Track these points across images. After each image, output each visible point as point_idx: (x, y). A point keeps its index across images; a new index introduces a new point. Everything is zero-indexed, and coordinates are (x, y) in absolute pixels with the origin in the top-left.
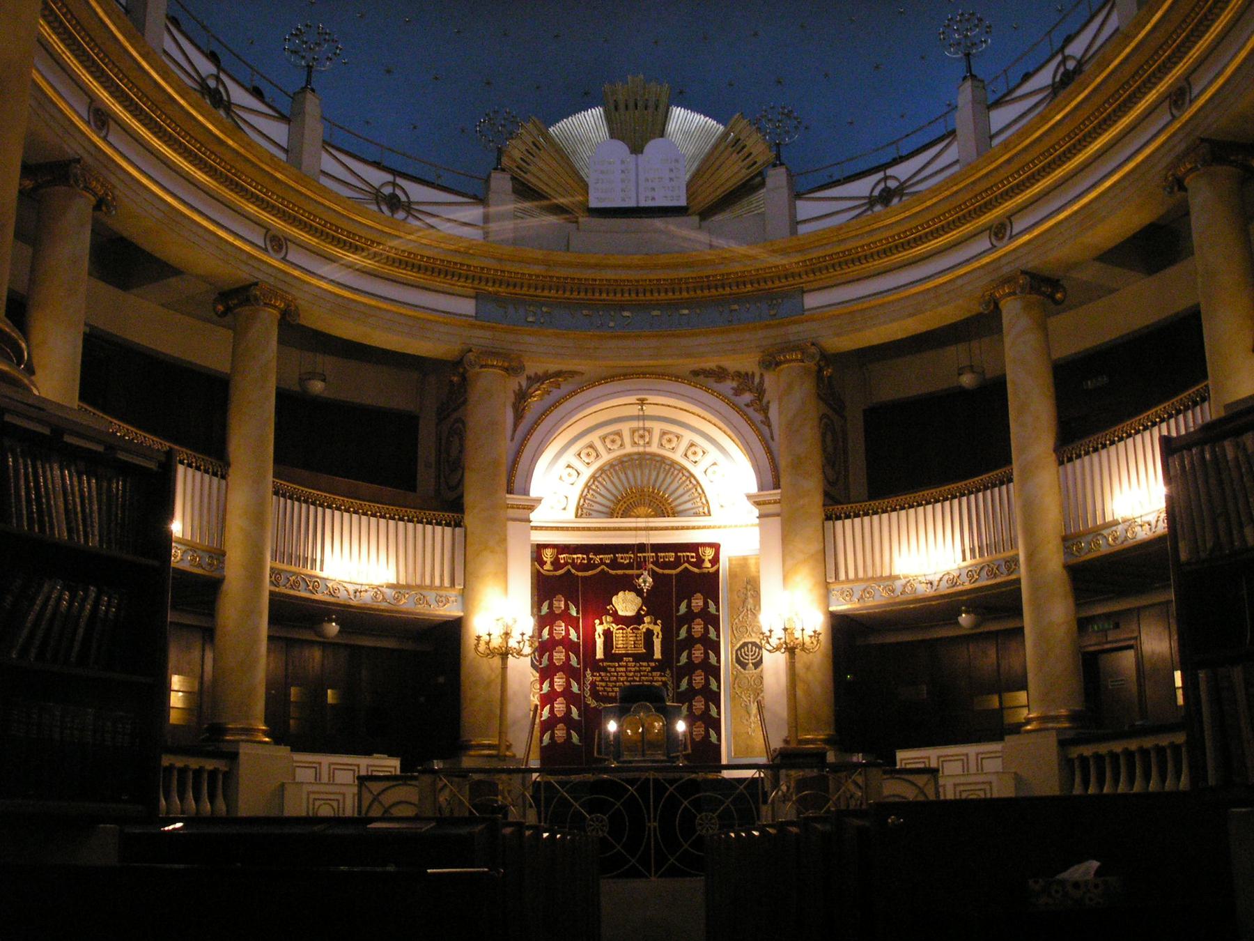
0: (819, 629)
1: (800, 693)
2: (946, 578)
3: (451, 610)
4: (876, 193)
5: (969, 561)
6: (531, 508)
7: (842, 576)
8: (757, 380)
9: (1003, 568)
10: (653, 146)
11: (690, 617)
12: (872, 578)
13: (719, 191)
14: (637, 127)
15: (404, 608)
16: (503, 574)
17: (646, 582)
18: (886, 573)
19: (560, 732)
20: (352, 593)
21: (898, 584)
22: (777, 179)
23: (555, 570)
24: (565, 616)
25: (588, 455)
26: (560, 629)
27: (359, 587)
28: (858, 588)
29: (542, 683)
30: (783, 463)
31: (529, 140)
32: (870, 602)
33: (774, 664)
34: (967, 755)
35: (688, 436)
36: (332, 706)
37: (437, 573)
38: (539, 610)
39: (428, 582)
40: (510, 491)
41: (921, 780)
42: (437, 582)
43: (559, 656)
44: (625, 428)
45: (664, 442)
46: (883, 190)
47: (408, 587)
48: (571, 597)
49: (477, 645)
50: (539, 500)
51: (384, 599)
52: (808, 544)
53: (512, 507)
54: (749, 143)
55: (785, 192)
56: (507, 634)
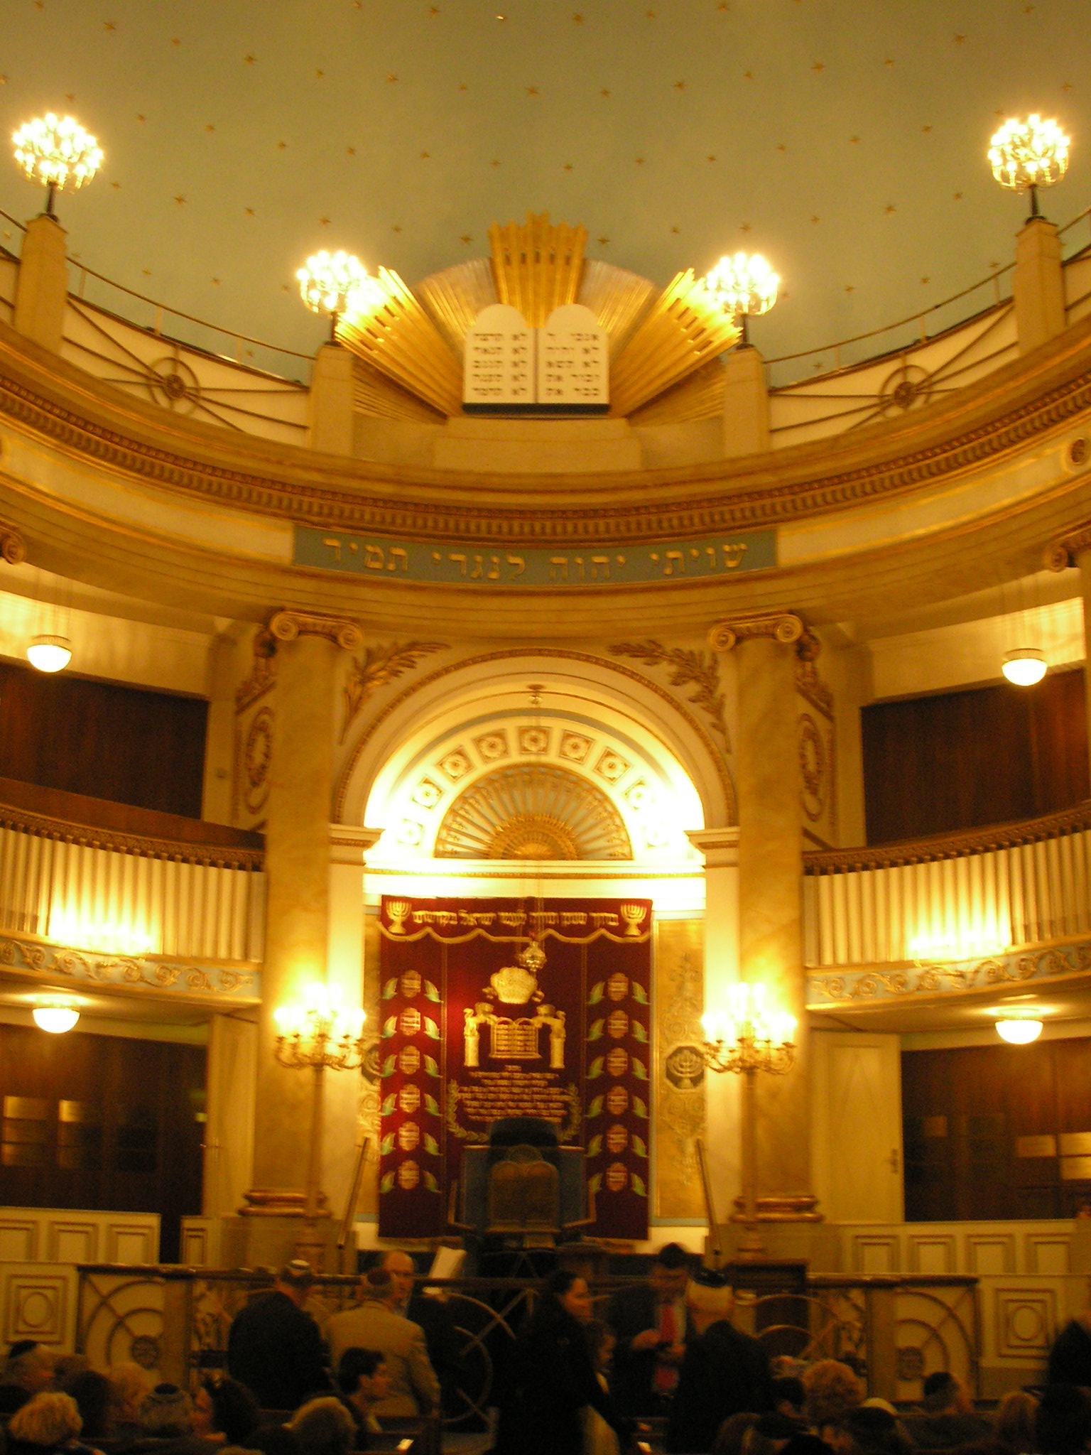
0: (791, 1040)
1: (760, 1132)
2: (987, 968)
3: (243, 995)
4: (890, 391)
5: (1022, 945)
6: (366, 844)
7: (828, 959)
8: (707, 662)
9: (1075, 959)
12: (873, 965)
13: (659, 382)
15: (171, 991)
16: (321, 941)
17: (535, 955)
18: (893, 958)
19: (408, 1174)
20: (92, 967)
21: (912, 974)
23: (407, 934)
24: (421, 1003)
25: (455, 765)
26: (413, 1020)
27: (101, 959)
28: (852, 976)
29: (383, 1100)
30: (743, 788)
32: (869, 1000)
33: (722, 1091)
34: (1010, 1236)
35: (603, 741)
36: (68, 1124)
37: (223, 937)
38: (382, 992)
39: (208, 952)
40: (336, 819)
41: (949, 1296)
42: (223, 953)
43: (410, 1059)
44: (510, 726)
45: (567, 748)
46: (901, 386)
47: (178, 960)
48: (429, 975)
49: (279, 1050)
50: (377, 834)
51: (142, 979)
52: (777, 909)
53: (339, 842)
56: (323, 1037)
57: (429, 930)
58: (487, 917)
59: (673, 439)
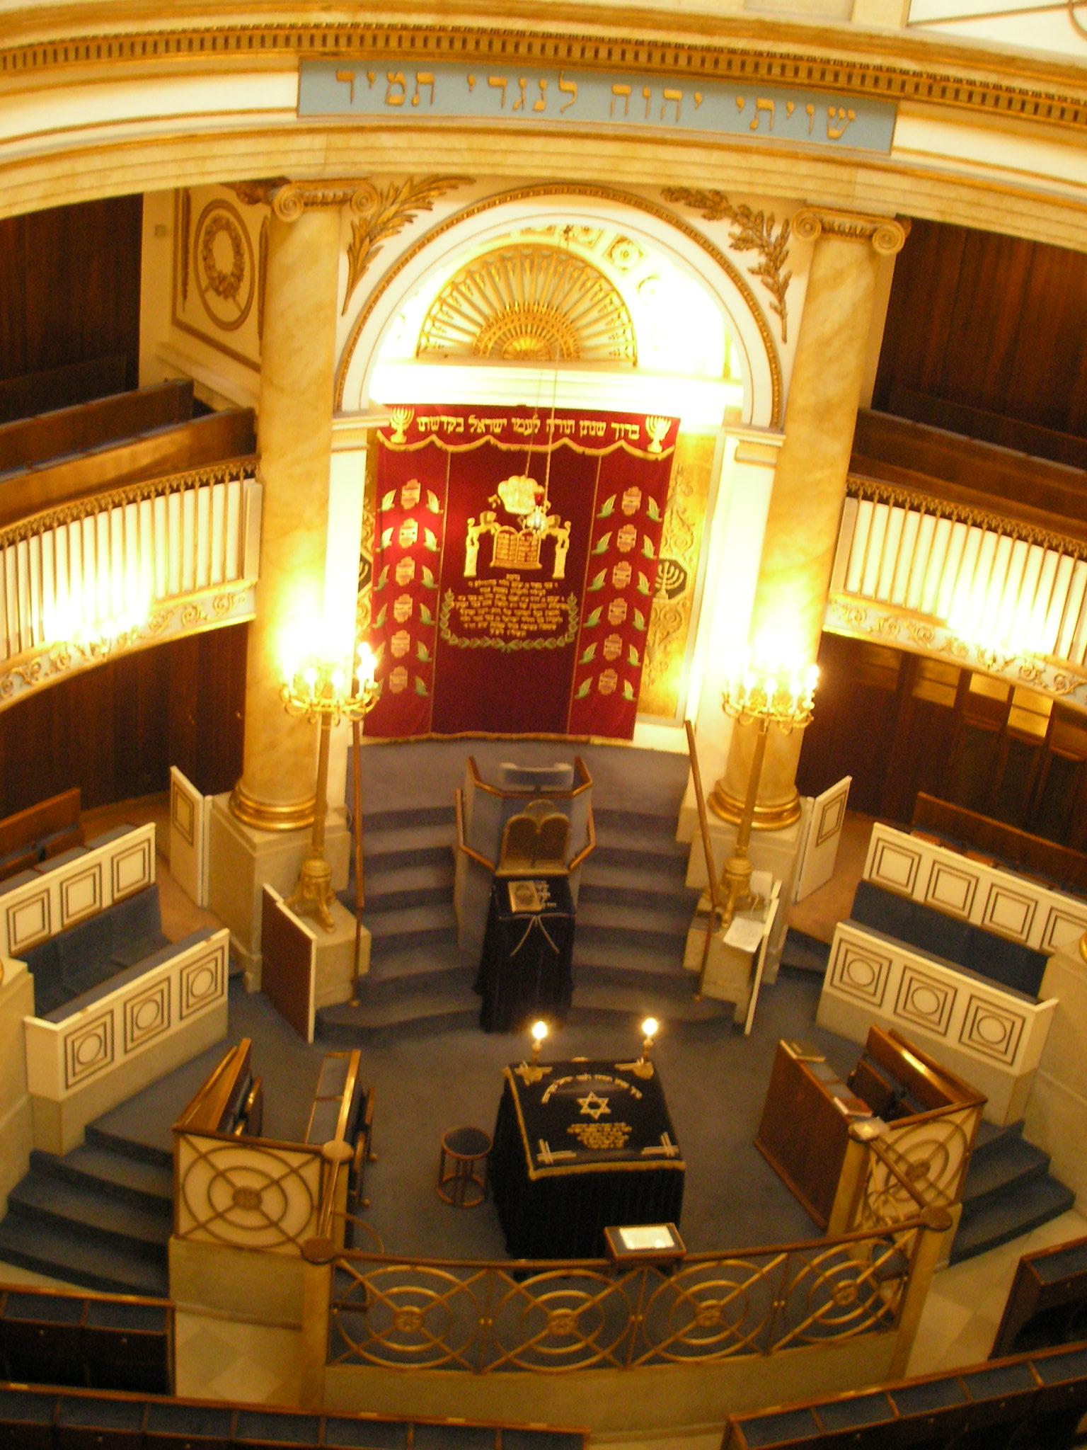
11: (618, 521)
24: (419, 511)
38: (379, 504)
57: (434, 438)
58: (497, 424)
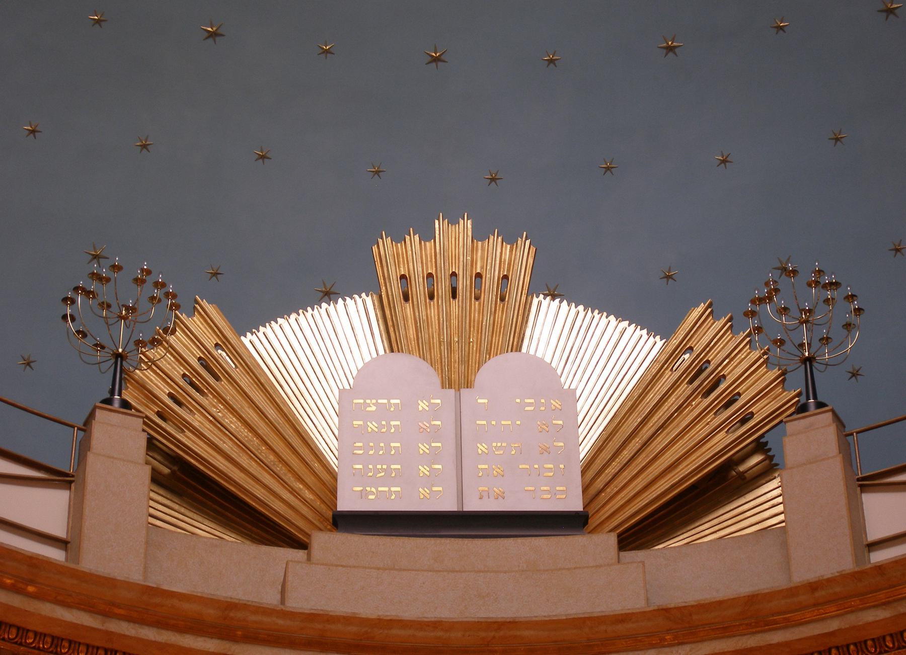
10: (494, 371)
14: (457, 342)
22: (810, 443)
31: (193, 356)
54: (732, 372)
55: (833, 472)
59: (705, 561)
